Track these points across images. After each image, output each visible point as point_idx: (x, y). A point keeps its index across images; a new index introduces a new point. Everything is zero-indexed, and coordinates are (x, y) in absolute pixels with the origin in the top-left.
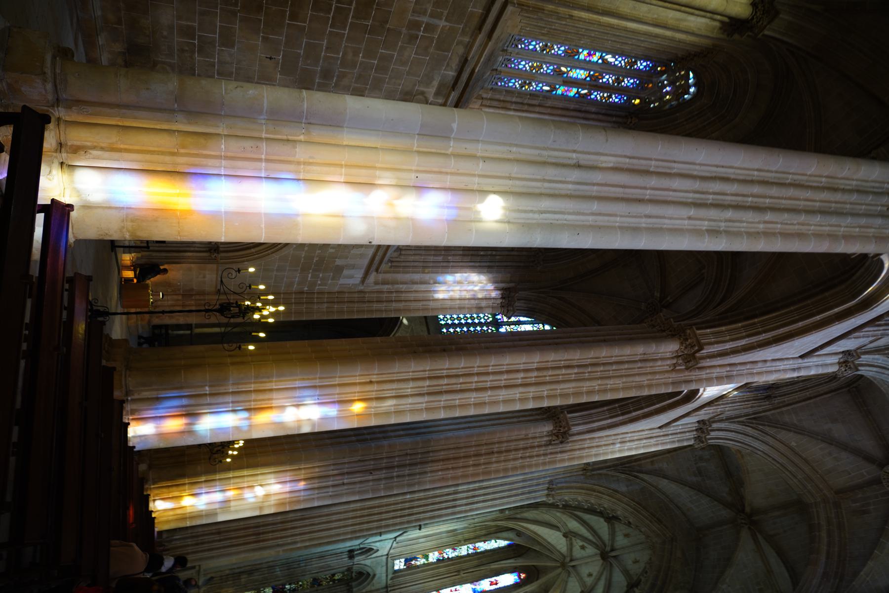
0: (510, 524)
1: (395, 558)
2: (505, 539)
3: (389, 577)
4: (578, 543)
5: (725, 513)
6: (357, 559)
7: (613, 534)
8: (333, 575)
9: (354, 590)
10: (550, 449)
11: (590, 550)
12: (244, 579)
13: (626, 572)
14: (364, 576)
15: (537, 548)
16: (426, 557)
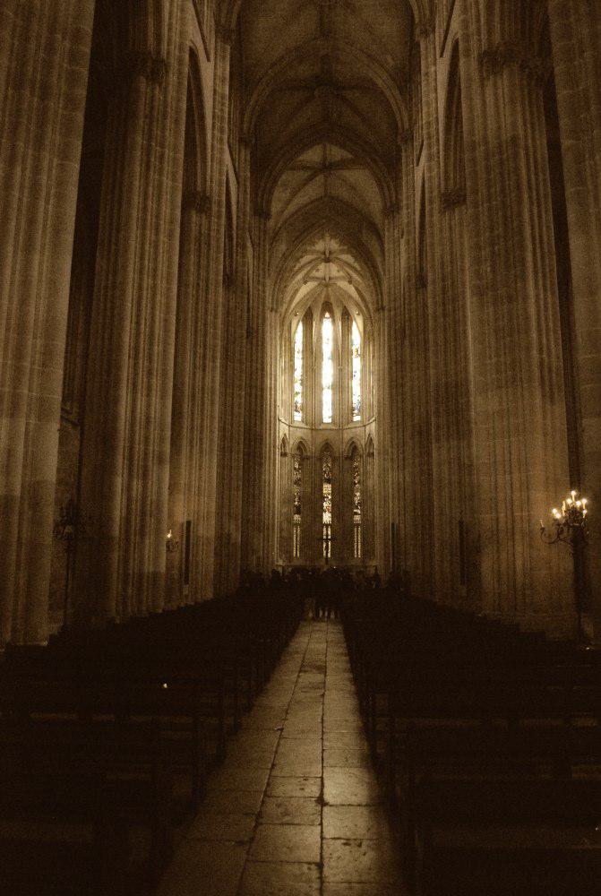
0: (287, 323)
1: (293, 421)
2: (297, 325)
3: (303, 425)
4: (314, 273)
5: (320, 179)
6: (288, 451)
7: (313, 252)
8: (295, 469)
9: (309, 454)
10: (254, 341)
11: (322, 266)
12: (285, 534)
13: (342, 252)
14: (301, 446)
15: (310, 303)
16: (297, 393)
